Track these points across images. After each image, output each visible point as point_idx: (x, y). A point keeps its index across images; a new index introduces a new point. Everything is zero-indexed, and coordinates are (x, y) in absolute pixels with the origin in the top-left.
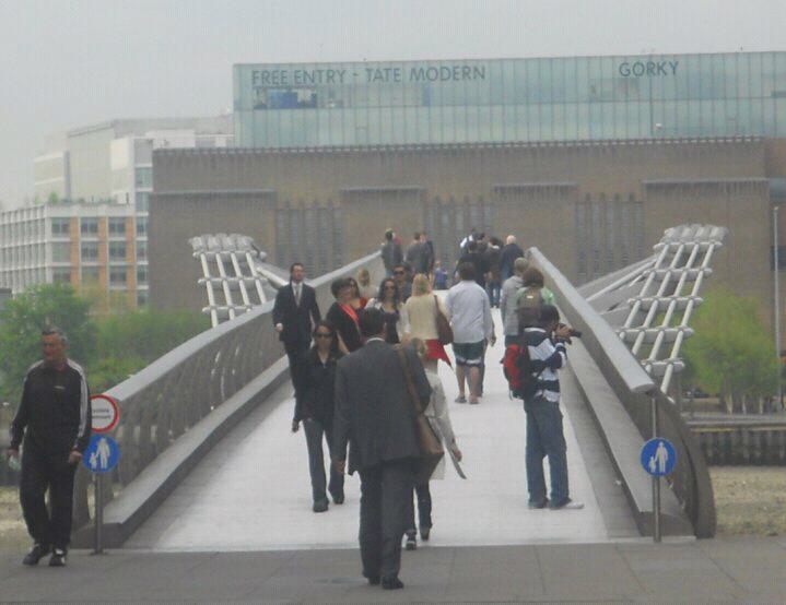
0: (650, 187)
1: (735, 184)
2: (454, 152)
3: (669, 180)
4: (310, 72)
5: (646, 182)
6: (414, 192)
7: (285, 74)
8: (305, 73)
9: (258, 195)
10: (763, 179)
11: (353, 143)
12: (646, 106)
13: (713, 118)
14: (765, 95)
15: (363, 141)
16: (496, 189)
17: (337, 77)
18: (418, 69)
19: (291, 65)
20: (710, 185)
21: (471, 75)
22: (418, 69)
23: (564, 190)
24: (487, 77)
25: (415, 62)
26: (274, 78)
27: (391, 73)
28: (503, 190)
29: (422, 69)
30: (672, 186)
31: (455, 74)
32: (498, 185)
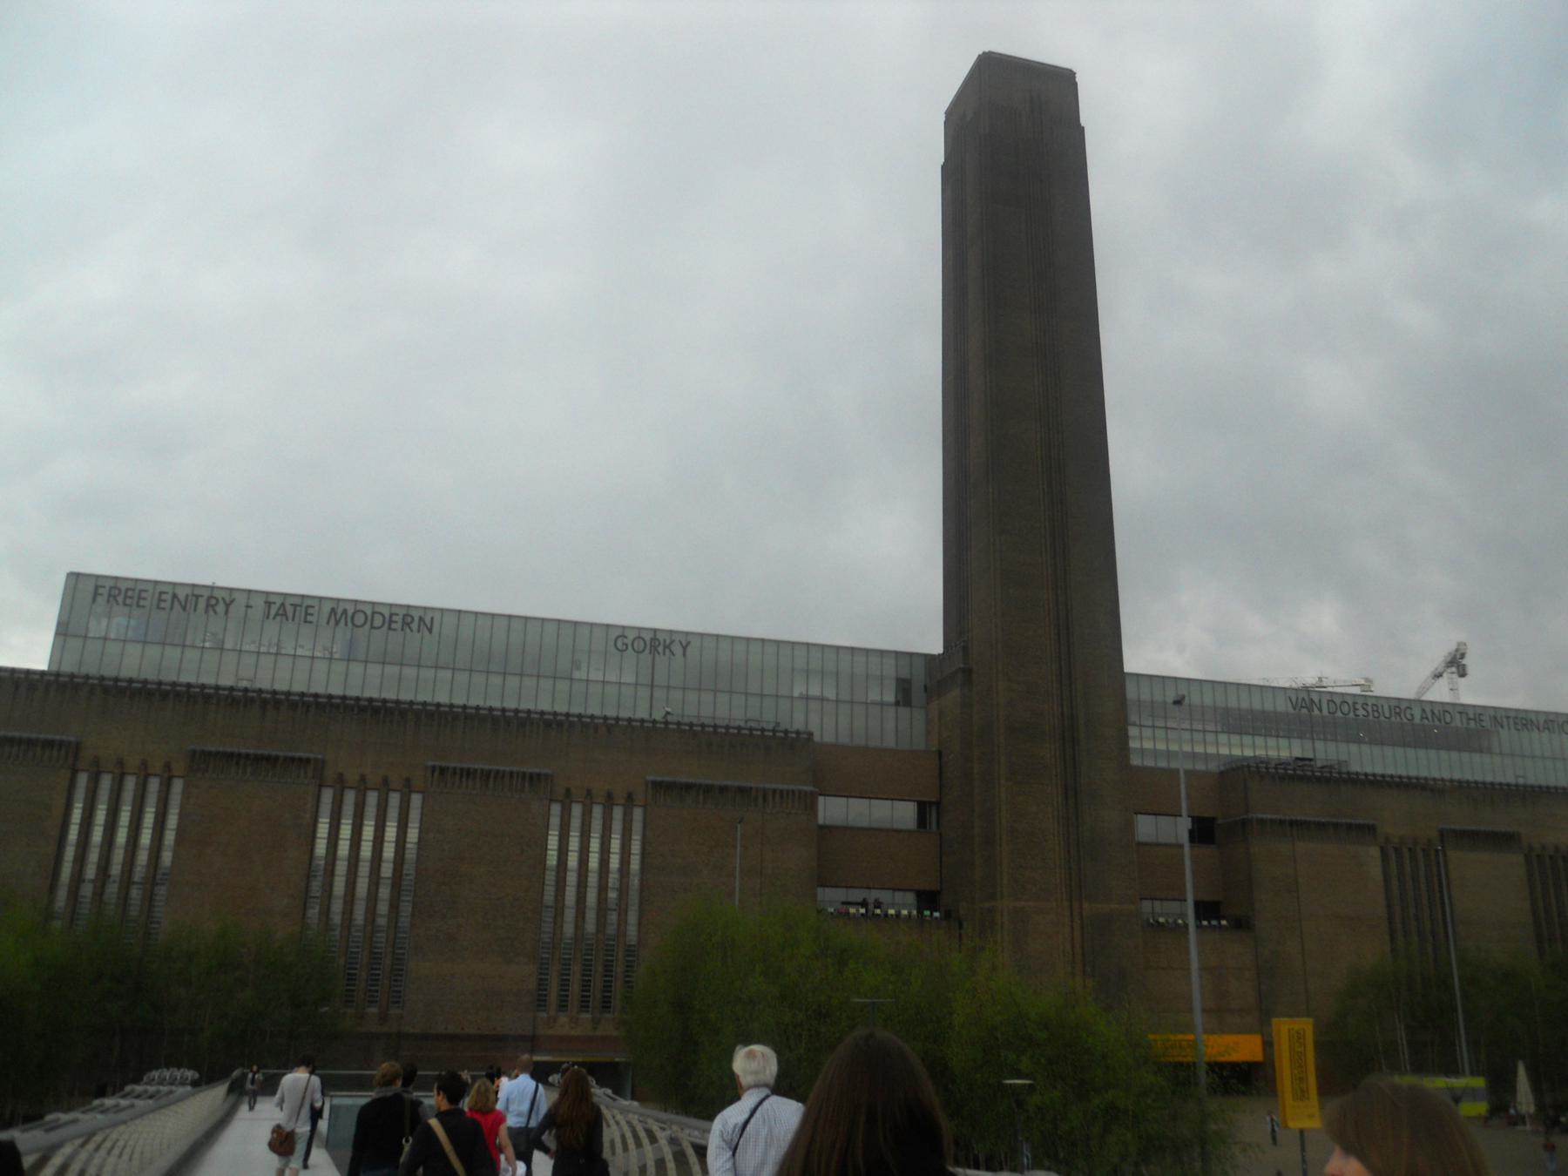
0: (657, 785)
1: (774, 791)
2: (376, 711)
3: (683, 779)
4: (181, 596)
5: (650, 778)
7: (144, 595)
8: (175, 596)
9: (48, 744)
10: (809, 788)
13: (727, 710)
16: (434, 768)
17: (221, 608)
18: (339, 611)
19: (156, 583)
21: (415, 626)
22: (339, 611)
23: (534, 779)
24: (436, 629)
25: (338, 600)
26: (126, 597)
27: (300, 613)
28: (443, 770)
29: (345, 611)
30: (688, 787)
31: (391, 621)
32: (437, 763)
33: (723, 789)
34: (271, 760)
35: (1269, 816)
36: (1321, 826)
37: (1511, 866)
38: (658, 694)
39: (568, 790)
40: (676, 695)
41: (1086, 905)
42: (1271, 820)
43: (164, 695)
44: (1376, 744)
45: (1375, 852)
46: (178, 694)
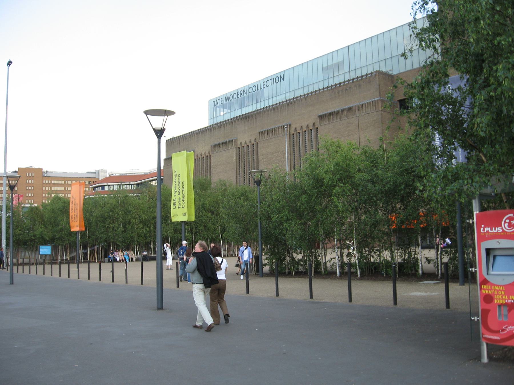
20: (350, 109)
30: (330, 114)
33: (343, 111)
39: (296, 129)
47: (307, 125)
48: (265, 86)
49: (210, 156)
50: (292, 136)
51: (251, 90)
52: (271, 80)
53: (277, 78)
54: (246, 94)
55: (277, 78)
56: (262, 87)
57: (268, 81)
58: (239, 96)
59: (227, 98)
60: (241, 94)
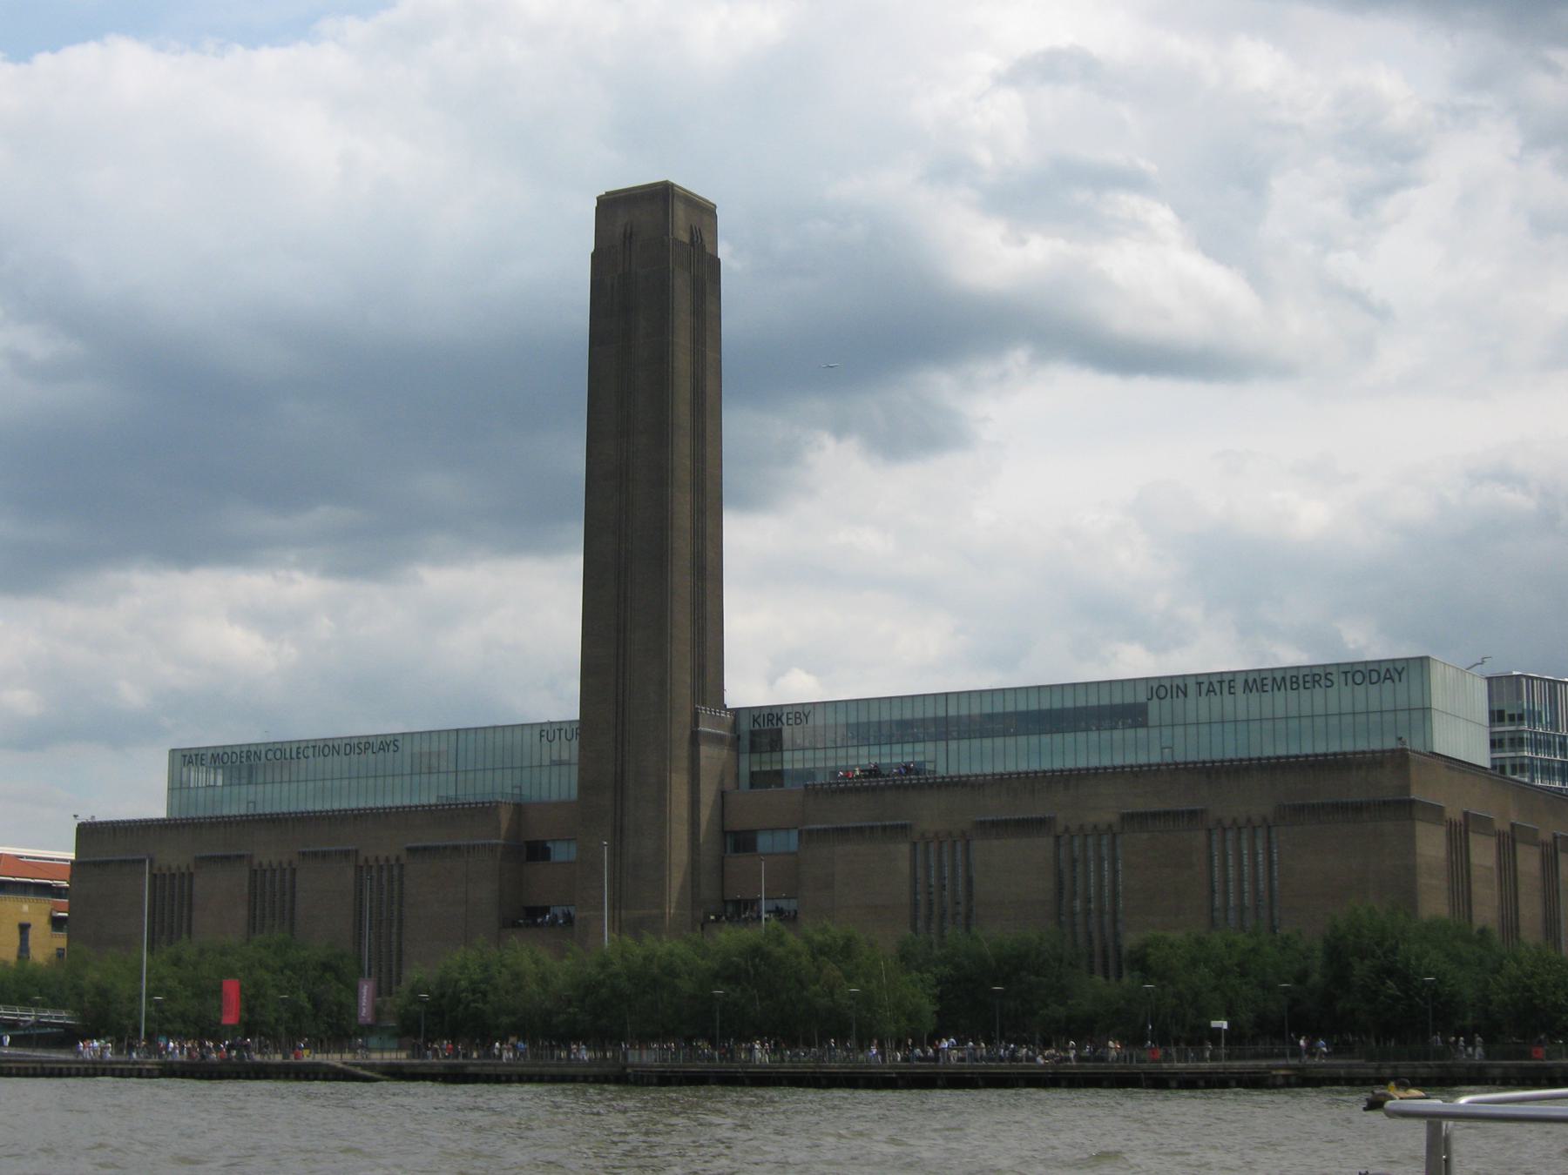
6: (240, 857)
11: (279, 811)
12: (452, 777)
14: (534, 764)
15: (251, 811)
16: (299, 853)
20: (456, 848)
28: (304, 854)
30: (425, 849)
33: (445, 848)
34: (227, 858)
35: (819, 826)
36: (860, 830)
37: (1041, 847)
38: (461, 777)
40: (471, 775)
41: (623, 911)
42: (818, 830)
43: (184, 825)
44: (998, 736)
45: (905, 848)
46: (189, 824)
47: (387, 857)
48: (301, 755)
49: (191, 874)
50: (359, 869)
51: (270, 755)
52: (314, 747)
53: (327, 748)
54: (260, 760)
55: (327, 748)
56: (294, 755)
57: (308, 747)
58: (244, 760)
59: (215, 755)
60: (248, 757)
